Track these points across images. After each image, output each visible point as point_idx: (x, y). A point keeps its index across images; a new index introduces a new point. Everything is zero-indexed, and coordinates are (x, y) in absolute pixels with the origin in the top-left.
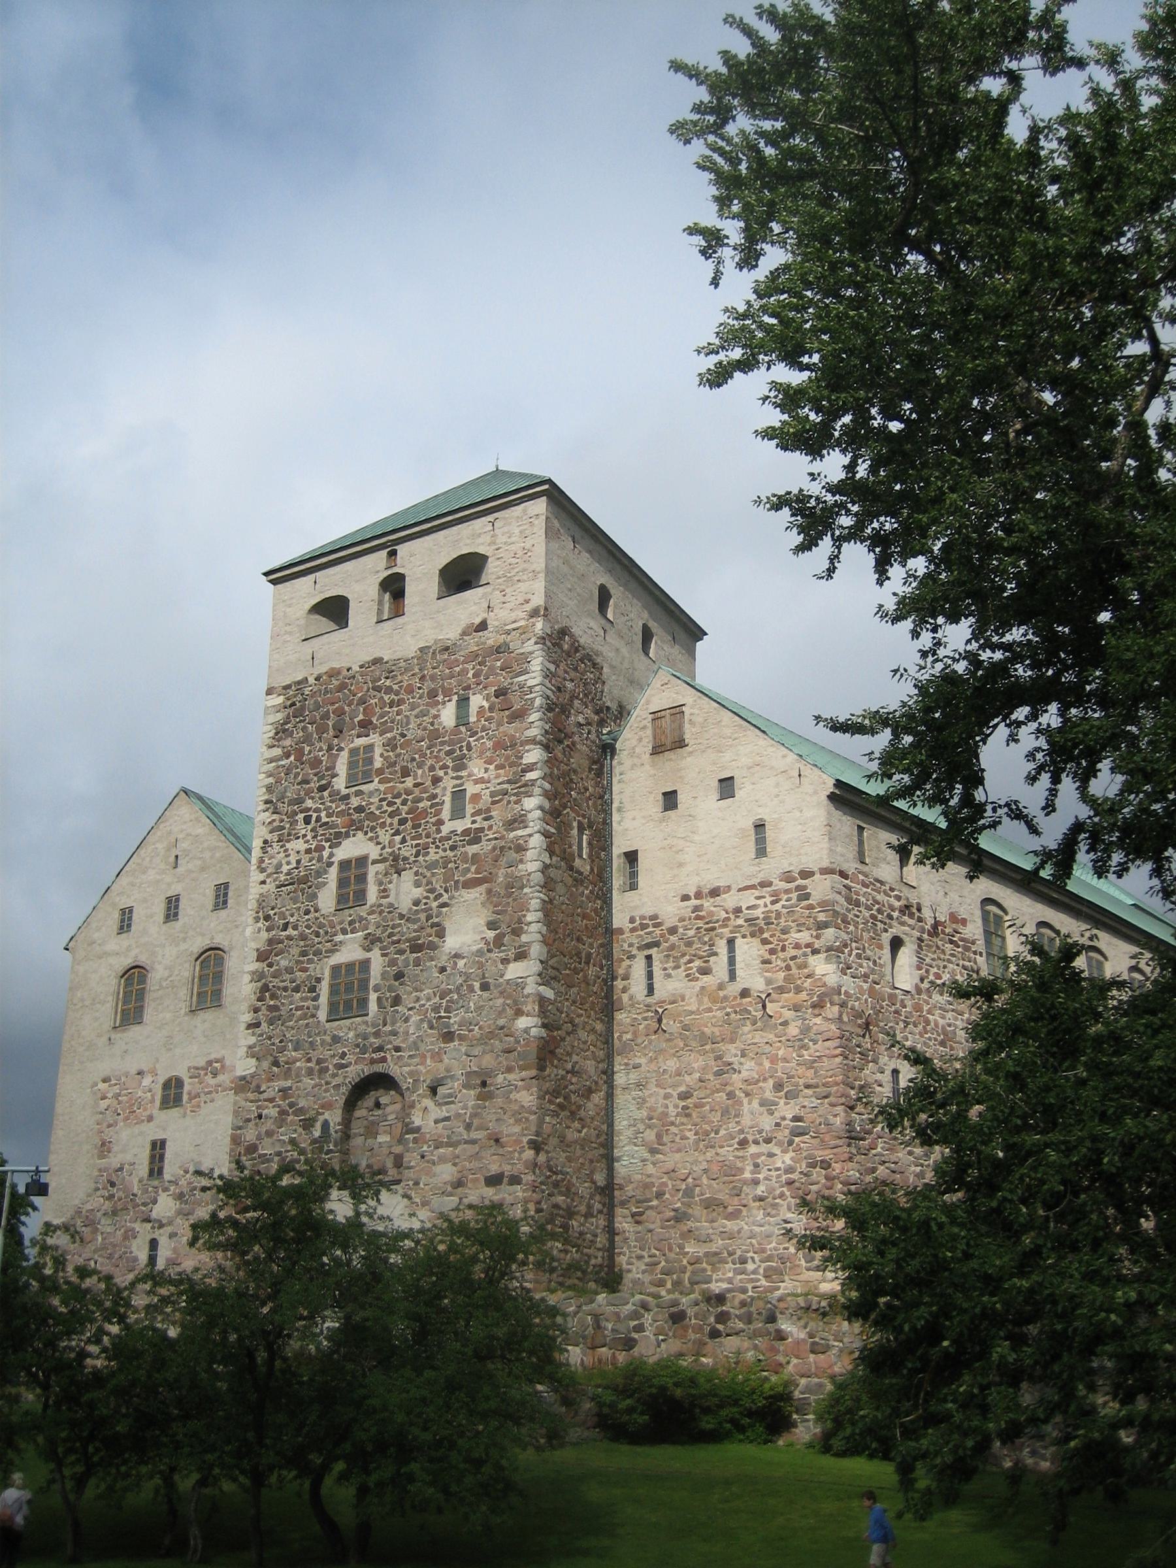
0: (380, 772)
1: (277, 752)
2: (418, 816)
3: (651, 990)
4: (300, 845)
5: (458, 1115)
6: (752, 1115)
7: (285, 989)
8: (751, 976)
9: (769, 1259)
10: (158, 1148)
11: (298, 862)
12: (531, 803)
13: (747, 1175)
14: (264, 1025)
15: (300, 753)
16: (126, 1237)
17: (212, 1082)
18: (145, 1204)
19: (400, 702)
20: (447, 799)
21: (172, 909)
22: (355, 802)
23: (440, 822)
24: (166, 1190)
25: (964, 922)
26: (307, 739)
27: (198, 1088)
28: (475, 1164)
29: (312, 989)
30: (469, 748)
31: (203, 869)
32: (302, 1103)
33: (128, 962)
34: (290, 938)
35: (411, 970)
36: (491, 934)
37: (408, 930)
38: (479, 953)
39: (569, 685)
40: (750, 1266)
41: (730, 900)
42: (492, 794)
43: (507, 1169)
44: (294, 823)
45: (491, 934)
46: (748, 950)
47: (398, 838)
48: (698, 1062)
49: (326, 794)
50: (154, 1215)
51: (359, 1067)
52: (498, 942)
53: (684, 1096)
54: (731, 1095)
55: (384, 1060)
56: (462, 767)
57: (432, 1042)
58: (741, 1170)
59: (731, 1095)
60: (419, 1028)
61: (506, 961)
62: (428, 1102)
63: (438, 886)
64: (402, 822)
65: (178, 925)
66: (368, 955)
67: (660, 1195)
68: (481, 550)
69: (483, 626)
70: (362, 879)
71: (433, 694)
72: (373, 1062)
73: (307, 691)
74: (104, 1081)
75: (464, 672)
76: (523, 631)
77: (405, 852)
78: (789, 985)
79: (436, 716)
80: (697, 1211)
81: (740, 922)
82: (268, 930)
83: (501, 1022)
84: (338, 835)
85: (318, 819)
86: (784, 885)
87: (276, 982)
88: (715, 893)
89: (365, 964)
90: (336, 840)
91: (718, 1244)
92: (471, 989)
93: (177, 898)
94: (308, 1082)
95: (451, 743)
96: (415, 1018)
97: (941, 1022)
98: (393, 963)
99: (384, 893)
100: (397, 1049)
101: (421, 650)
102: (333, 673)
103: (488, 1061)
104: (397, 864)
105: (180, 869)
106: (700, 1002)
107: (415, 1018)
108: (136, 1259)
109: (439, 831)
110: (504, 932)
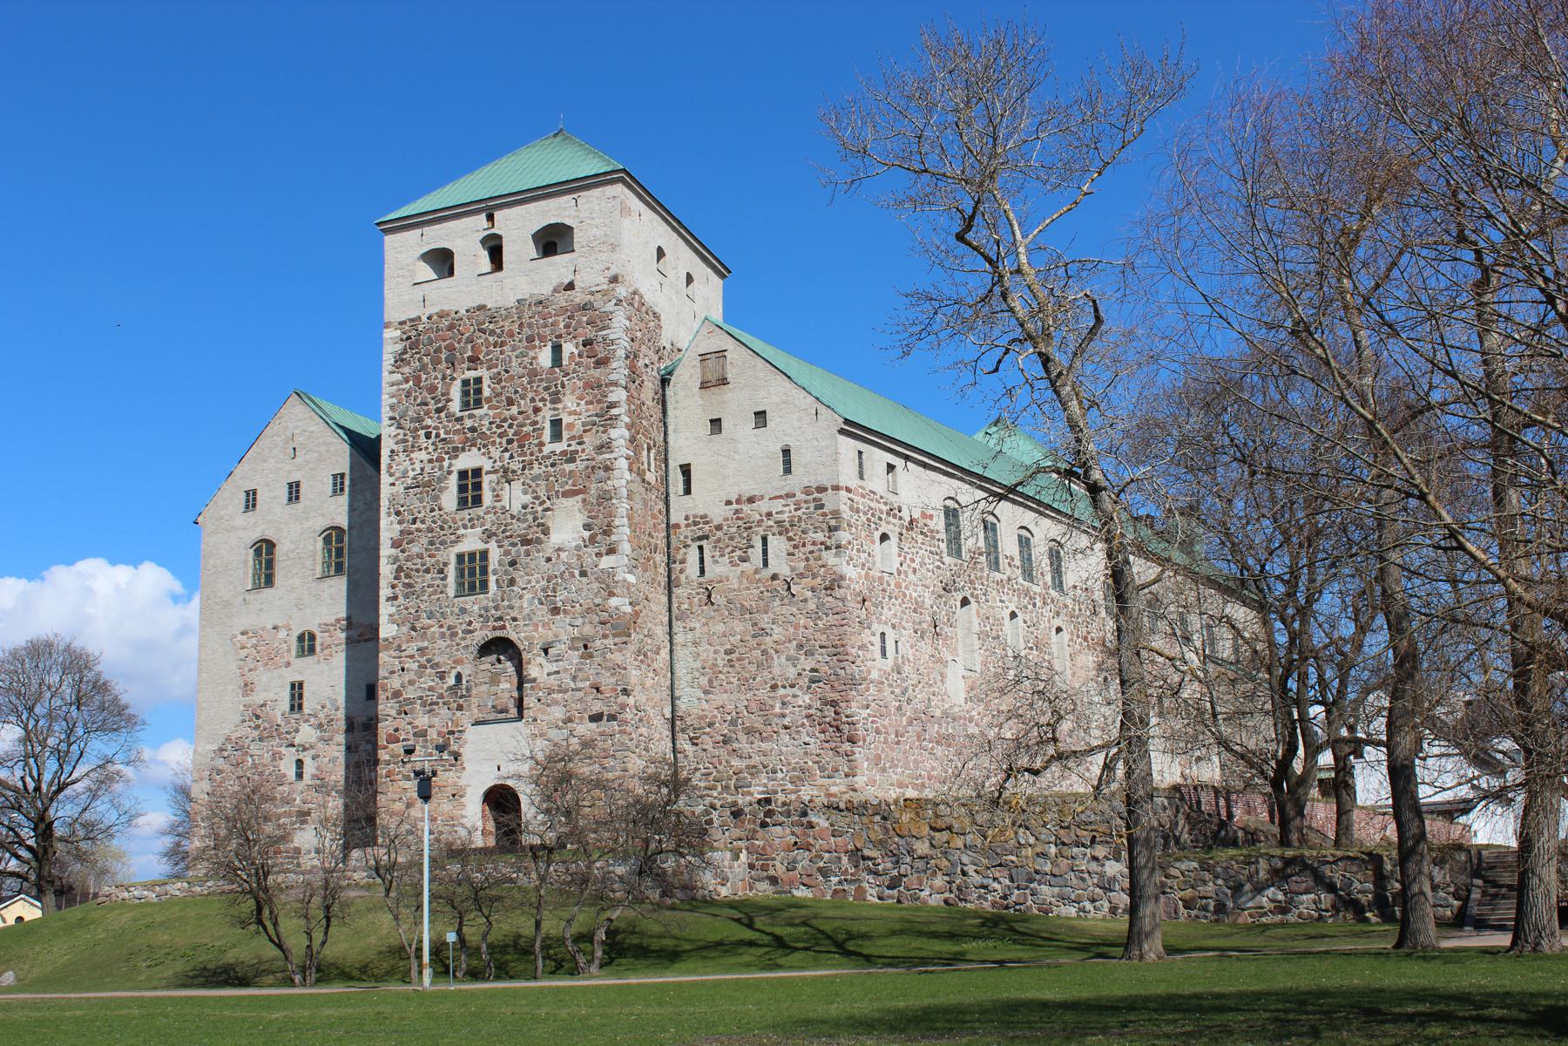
0: (489, 400)
1: (398, 377)
2: (522, 439)
3: (702, 571)
4: (423, 455)
5: (566, 670)
6: (782, 668)
7: (418, 571)
8: (780, 564)
9: (794, 769)
10: (297, 689)
12: (619, 434)
13: (777, 710)
14: (401, 599)
15: (417, 381)
16: (274, 759)
19: (503, 344)
20: (547, 425)
21: (294, 492)
22: (468, 423)
23: (541, 444)
25: (931, 517)
27: (328, 641)
29: (441, 571)
30: (563, 386)
31: (319, 460)
32: (437, 659)
33: (256, 536)
34: (419, 530)
35: (523, 560)
36: (587, 534)
37: (518, 528)
38: (578, 548)
39: (639, 334)
40: (780, 775)
41: (764, 506)
44: (416, 437)
46: (777, 545)
47: (507, 455)
48: (739, 627)
49: (443, 415)
50: (297, 741)
52: (592, 540)
53: (727, 652)
54: (764, 652)
55: (503, 627)
56: (558, 401)
57: (542, 613)
58: (772, 707)
59: (764, 652)
60: (531, 603)
61: (599, 555)
62: (541, 659)
63: (542, 493)
64: (510, 442)
65: (299, 506)
67: (711, 725)
68: (567, 222)
69: (570, 286)
70: (478, 486)
71: (530, 339)
72: (495, 628)
74: (243, 634)
76: (605, 293)
78: (809, 572)
79: (534, 358)
80: (743, 737)
81: (771, 523)
82: (400, 523)
83: (597, 601)
84: (455, 449)
85: (438, 435)
86: (804, 497)
88: (751, 500)
89: (484, 555)
90: (455, 452)
91: (756, 760)
93: (298, 484)
94: (441, 643)
95: (548, 380)
96: (528, 596)
97: (915, 595)
98: (507, 553)
99: (498, 498)
100: (514, 619)
102: (441, 315)
103: (588, 630)
104: (507, 476)
105: (298, 460)
106: (741, 582)
107: (528, 596)
108: (284, 776)
109: (541, 451)
110: (599, 533)
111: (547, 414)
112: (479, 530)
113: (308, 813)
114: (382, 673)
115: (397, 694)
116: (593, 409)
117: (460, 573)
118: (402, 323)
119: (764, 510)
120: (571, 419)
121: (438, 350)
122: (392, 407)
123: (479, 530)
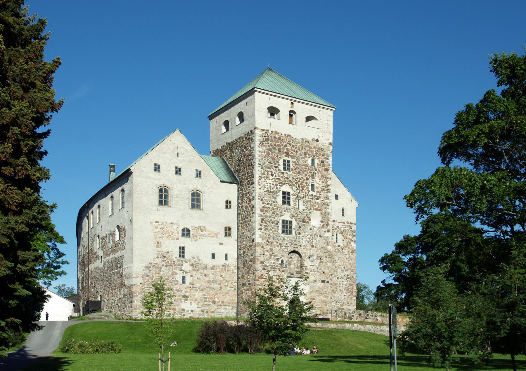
0: (292, 170)
4: (270, 181)
11: (270, 186)
14: (263, 230)
17: (202, 233)
18: (179, 265)
19: (297, 152)
22: (286, 176)
24: (186, 262)
26: (270, 150)
27: (195, 234)
28: (319, 277)
29: (277, 224)
31: (190, 161)
34: (269, 208)
35: (302, 227)
36: (322, 224)
37: (302, 217)
42: (321, 189)
43: (327, 280)
45: (322, 224)
47: (298, 191)
49: (277, 169)
51: (291, 248)
52: (323, 225)
54: (336, 267)
55: (297, 248)
56: (313, 178)
57: (308, 246)
59: (336, 267)
62: (308, 260)
64: (299, 186)
66: (290, 219)
69: (317, 140)
71: (305, 153)
72: (294, 247)
73: (269, 134)
74: (156, 222)
75: (313, 151)
77: (300, 195)
79: (307, 161)
82: (263, 203)
84: (281, 183)
85: (275, 176)
87: (266, 219)
89: (291, 222)
90: (281, 184)
92: (317, 236)
94: (277, 249)
96: (304, 240)
98: (298, 224)
100: (300, 246)
101: (302, 139)
102: (277, 133)
103: (322, 254)
104: (298, 198)
108: (177, 281)
111: (310, 182)
112: (289, 213)
113: (186, 297)
114: (257, 254)
115: (262, 263)
116: (324, 184)
117: (283, 227)
118: (262, 130)
119: (337, 225)
120: (318, 185)
121: (275, 145)
122: (259, 160)
123: (289, 213)
